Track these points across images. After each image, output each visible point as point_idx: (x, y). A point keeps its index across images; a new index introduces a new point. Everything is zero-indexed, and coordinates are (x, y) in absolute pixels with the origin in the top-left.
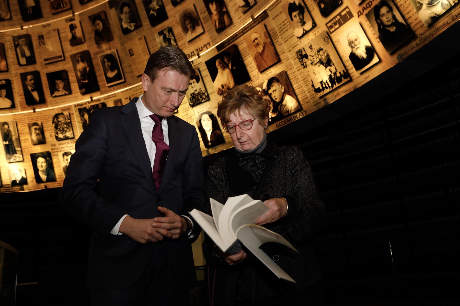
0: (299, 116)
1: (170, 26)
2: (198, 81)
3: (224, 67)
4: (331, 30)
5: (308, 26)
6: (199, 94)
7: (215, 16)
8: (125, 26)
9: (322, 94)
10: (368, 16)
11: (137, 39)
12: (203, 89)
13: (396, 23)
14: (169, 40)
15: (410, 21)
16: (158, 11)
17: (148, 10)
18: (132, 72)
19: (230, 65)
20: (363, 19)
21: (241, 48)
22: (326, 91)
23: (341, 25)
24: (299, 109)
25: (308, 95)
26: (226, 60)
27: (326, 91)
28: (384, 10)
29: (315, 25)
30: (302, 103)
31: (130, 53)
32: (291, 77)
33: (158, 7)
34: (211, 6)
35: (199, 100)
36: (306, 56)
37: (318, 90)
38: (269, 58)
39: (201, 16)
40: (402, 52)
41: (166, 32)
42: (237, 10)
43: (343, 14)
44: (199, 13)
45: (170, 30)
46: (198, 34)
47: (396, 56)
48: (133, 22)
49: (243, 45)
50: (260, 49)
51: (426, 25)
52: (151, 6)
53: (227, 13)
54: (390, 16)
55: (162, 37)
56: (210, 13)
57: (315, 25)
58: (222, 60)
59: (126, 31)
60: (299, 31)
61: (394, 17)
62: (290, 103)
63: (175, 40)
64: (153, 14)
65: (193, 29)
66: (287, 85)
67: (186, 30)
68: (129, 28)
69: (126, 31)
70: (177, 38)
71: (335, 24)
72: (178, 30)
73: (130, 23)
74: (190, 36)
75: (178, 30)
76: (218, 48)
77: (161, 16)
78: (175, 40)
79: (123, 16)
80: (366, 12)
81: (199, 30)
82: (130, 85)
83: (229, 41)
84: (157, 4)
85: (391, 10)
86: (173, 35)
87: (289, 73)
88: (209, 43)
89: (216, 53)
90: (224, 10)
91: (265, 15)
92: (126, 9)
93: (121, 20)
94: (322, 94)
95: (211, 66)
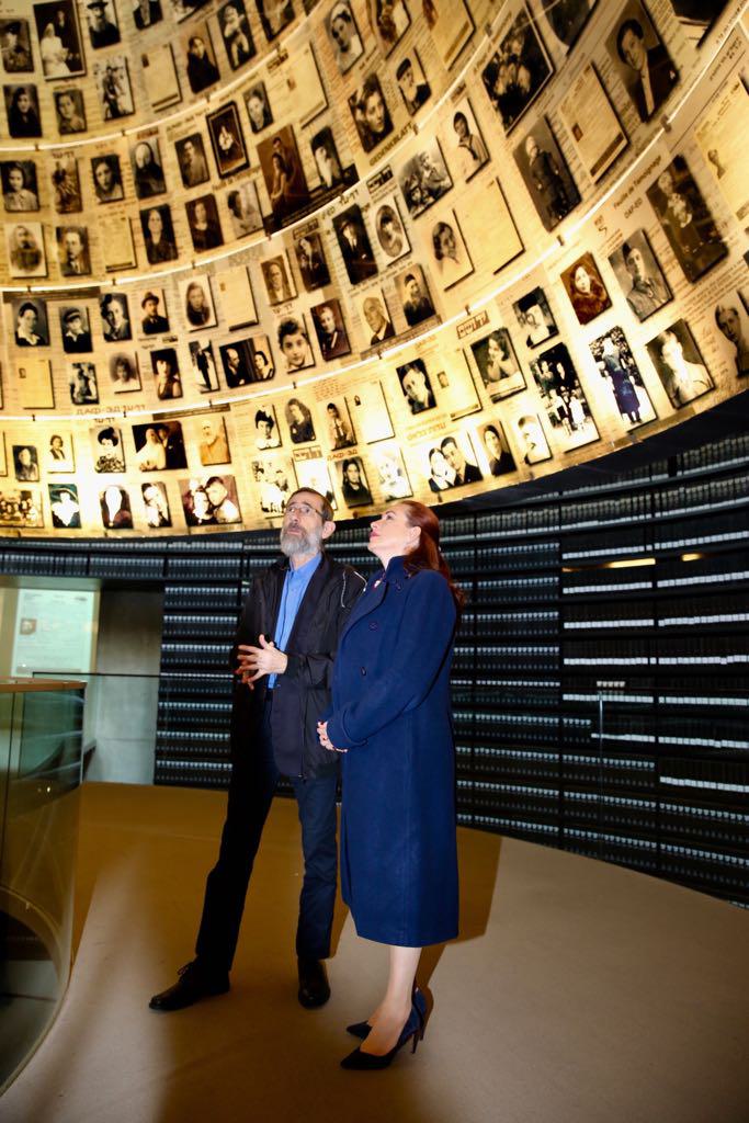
0: (237, 528)
1: (93, 362)
2: (115, 443)
3: (158, 440)
4: (298, 458)
5: (274, 442)
6: (112, 460)
7: (162, 378)
8: (22, 334)
9: (269, 515)
10: (337, 464)
11: (37, 358)
12: (120, 458)
13: (360, 484)
14: (87, 379)
15: (372, 489)
16: (79, 336)
17: (64, 331)
18: (16, 399)
19: (165, 442)
20: (332, 465)
21: (185, 429)
22: (274, 514)
23: (308, 458)
24: (239, 521)
25: (254, 511)
26: (161, 434)
27: (274, 514)
28: (352, 467)
29: (280, 445)
30: (243, 516)
31: (21, 373)
32: (238, 484)
33: (80, 332)
34: (159, 364)
35: (110, 467)
36: (262, 471)
37: (265, 510)
38: (218, 453)
39: (142, 370)
40: (358, 510)
41: (85, 368)
42: (192, 385)
43: (313, 449)
44: (140, 365)
45: (92, 368)
46: (132, 389)
47: (352, 511)
48: (36, 334)
49: (189, 427)
50: (210, 440)
51: (383, 500)
52: (71, 325)
53: (179, 382)
54: (356, 475)
55: (77, 371)
56: (156, 372)
57: (280, 445)
58: (157, 432)
59: (22, 342)
60: (263, 442)
61: (360, 478)
62: (228, 512)
63: (96, 383)
64: (71, 338)
65: (127, 379)
66: (231, 491)
67: (115, 377)
68: (28, 340)
69: (22, 342)
70: (99, 381)
71: (303, 454)
72: (103, 372)
73: (32, 333)
74: (120, 385)
75: (103, 372)
76: (156, 416)
77: (82, 344)
78: (96, 383)
79: (22, 321)
80: (336, 460)
81: (133, 384)
82: (8, 414)
83: (172, 415)
84: (82, 328)
85: (358, 470)
86: (95, 375)
87: (237, 479)
88: (143, 406)
89: (150, 421)
90: (176, 377)
91: (226, 408)
92: (29, 313)
93: (17, 325)
94: (269, 515)
95: (139, 433)
